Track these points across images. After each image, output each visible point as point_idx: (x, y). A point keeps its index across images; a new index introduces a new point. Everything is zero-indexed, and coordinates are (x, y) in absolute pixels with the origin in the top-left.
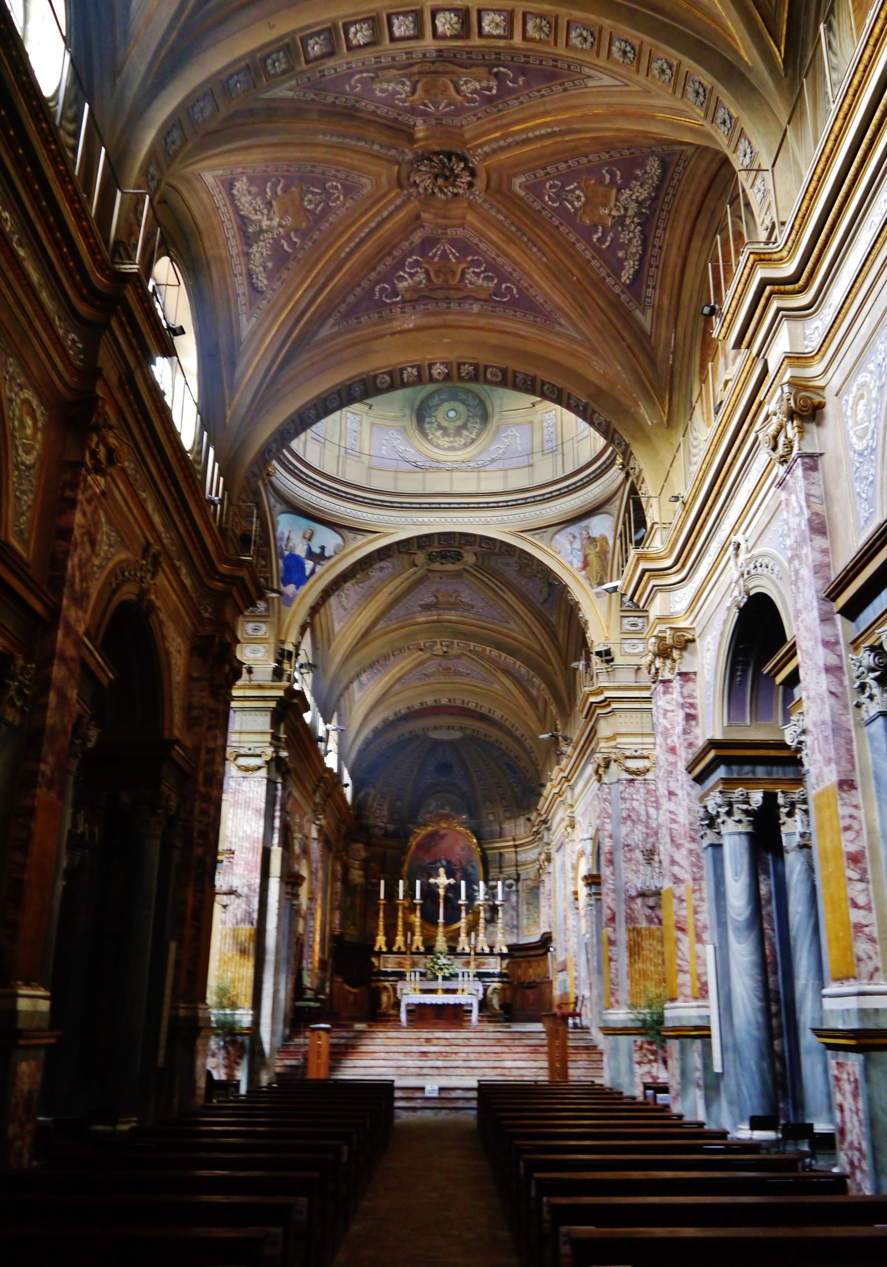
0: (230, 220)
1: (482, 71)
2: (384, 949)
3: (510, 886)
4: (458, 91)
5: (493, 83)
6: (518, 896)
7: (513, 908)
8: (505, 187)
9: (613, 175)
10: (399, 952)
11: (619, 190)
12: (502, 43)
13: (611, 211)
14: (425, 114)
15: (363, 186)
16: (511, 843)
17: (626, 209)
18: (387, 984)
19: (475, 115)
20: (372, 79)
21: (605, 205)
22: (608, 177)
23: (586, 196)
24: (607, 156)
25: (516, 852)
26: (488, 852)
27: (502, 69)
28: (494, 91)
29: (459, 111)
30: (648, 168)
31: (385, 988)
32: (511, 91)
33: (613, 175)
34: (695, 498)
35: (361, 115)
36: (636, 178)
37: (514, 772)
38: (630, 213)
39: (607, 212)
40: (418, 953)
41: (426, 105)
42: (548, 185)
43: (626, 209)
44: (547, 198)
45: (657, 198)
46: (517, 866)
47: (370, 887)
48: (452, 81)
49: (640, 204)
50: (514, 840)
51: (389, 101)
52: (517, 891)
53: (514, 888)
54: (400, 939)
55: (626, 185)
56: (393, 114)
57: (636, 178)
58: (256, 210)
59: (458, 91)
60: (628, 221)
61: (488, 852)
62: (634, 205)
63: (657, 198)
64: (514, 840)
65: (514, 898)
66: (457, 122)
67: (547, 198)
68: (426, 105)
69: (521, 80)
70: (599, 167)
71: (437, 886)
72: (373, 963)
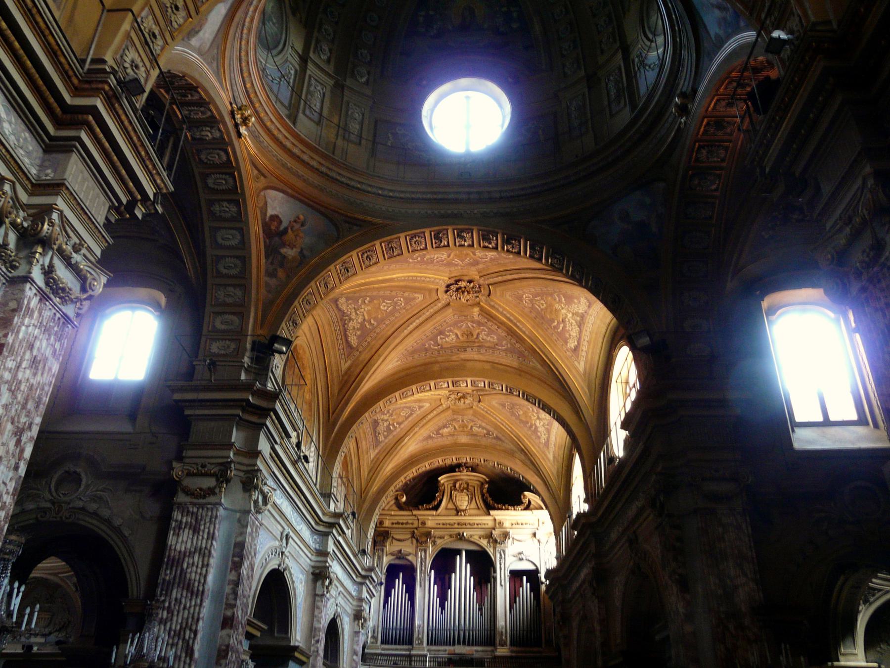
0: (586, 331)
1: (444, 346)
4: (457, 335)
5: (439, 341)
8: (427, 294)
9: (370, 323)
11: (364, 320)
12: (438, 380)
13: (364, 310)
14: (473, 322)
15: (511, 296)
17: (356, 314)
19: (447, 323)
20: (497, 345)
21: (369, 311)
22: (372, 322)
23: (380, 309)
24: (377, 331)
27: (436, 348)
28: (439, 338)
29: (455, 324)
30: (355, 338)
32: (431, 340)
33: (370, 323)
34: (296, 469)
35: (505, 329)
36: (358, 329)
38: (354, 314)
39: (366, 309)
41: (473, 326)
42: (403, 304)
43: (356, 314)
44: (402, 299)
45: (344, 326)
48: (459, 339)
49: (350, 319)
51: (491, 332)
55: (362, 325)
56: (490, 323)
57: (358, 329)
58: (572, 325)
59: (457, 335)
60: (353, 311)
62: (353, 317)
63: (344, 326)
66: (456, 318)
67: (402, 299)
68: (473, 326)
69: (427, 345)
70: (378, 324)
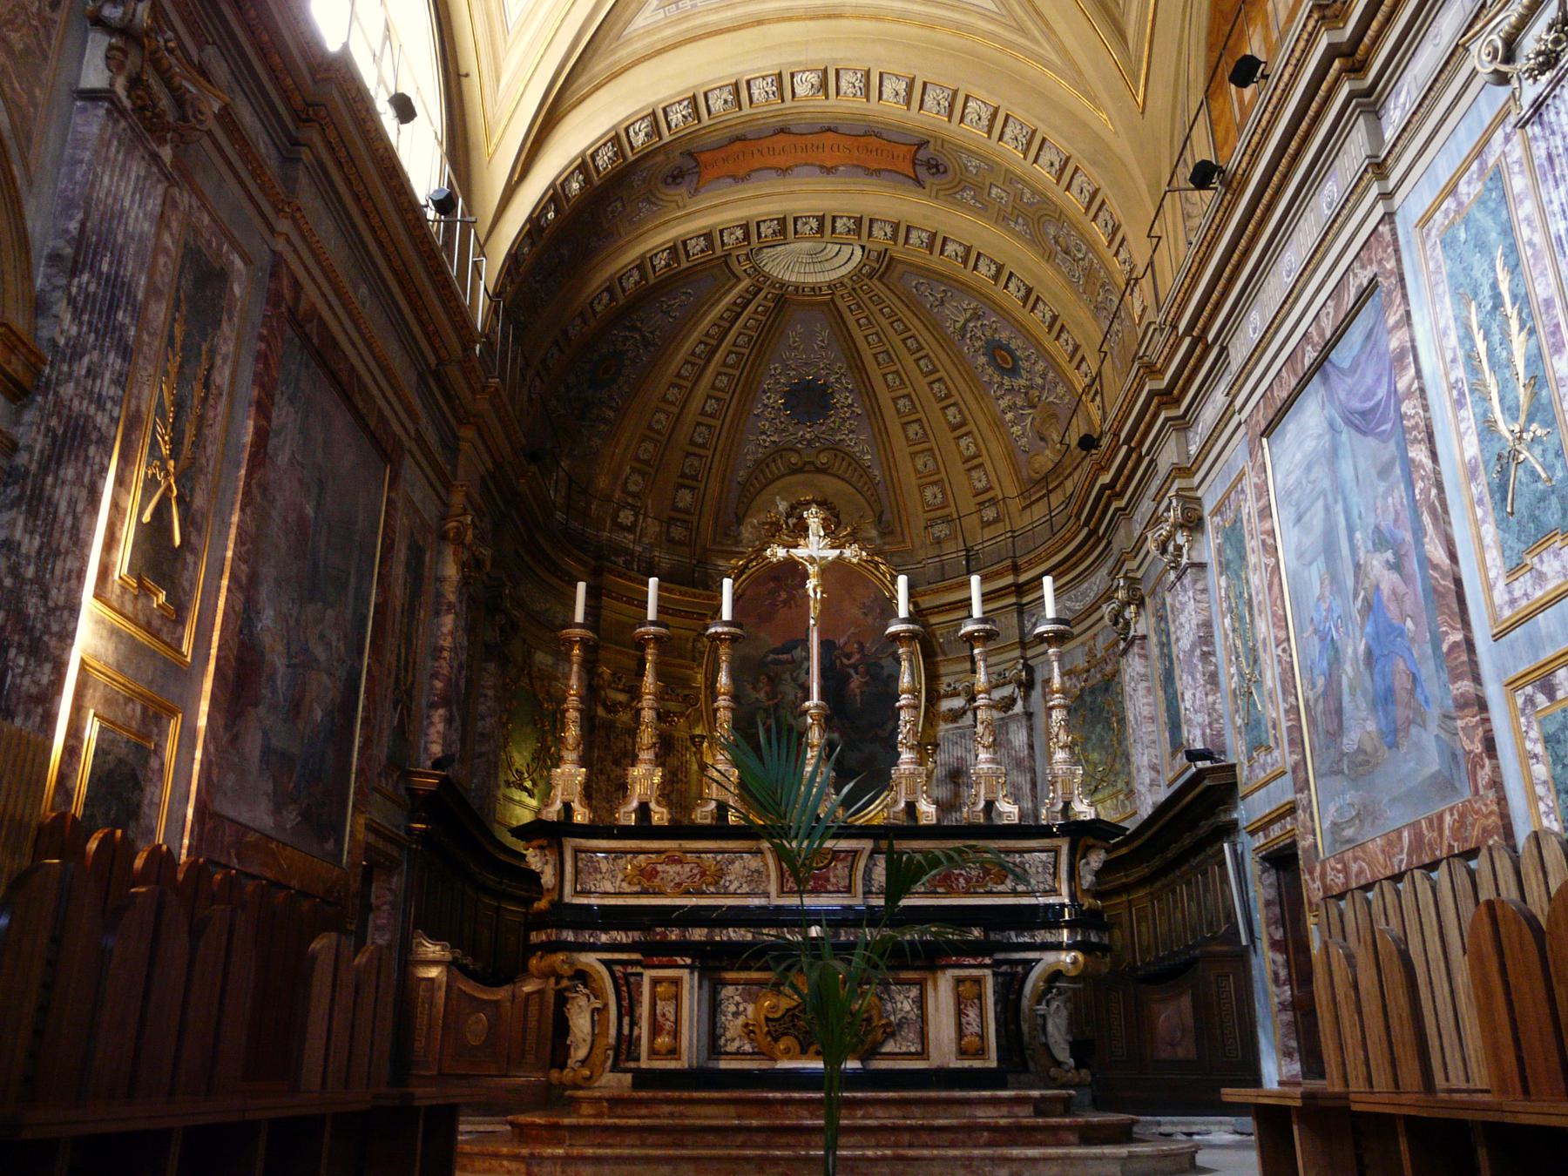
2: (581, 816)
3: (1008, 703)
6: (1031, 729)
7: (1018, 764)
10: (644, 829)
16: (1009, 580)
18: (590, 959)
25: (1021, 612)
26: (933, 620)
31: (582, 976)
37: (1014, 371)
40: (719, 830)
46: (1023, 645)
47: (601, 712)
50: (1016, 569)
52: (1029, 715)
53: (1019, 708)
54: (644, 778)
61: (933, 620)
64: (1016, 569)
65: (1019, 737)
71: (793, 572)
72: (535, 877)
